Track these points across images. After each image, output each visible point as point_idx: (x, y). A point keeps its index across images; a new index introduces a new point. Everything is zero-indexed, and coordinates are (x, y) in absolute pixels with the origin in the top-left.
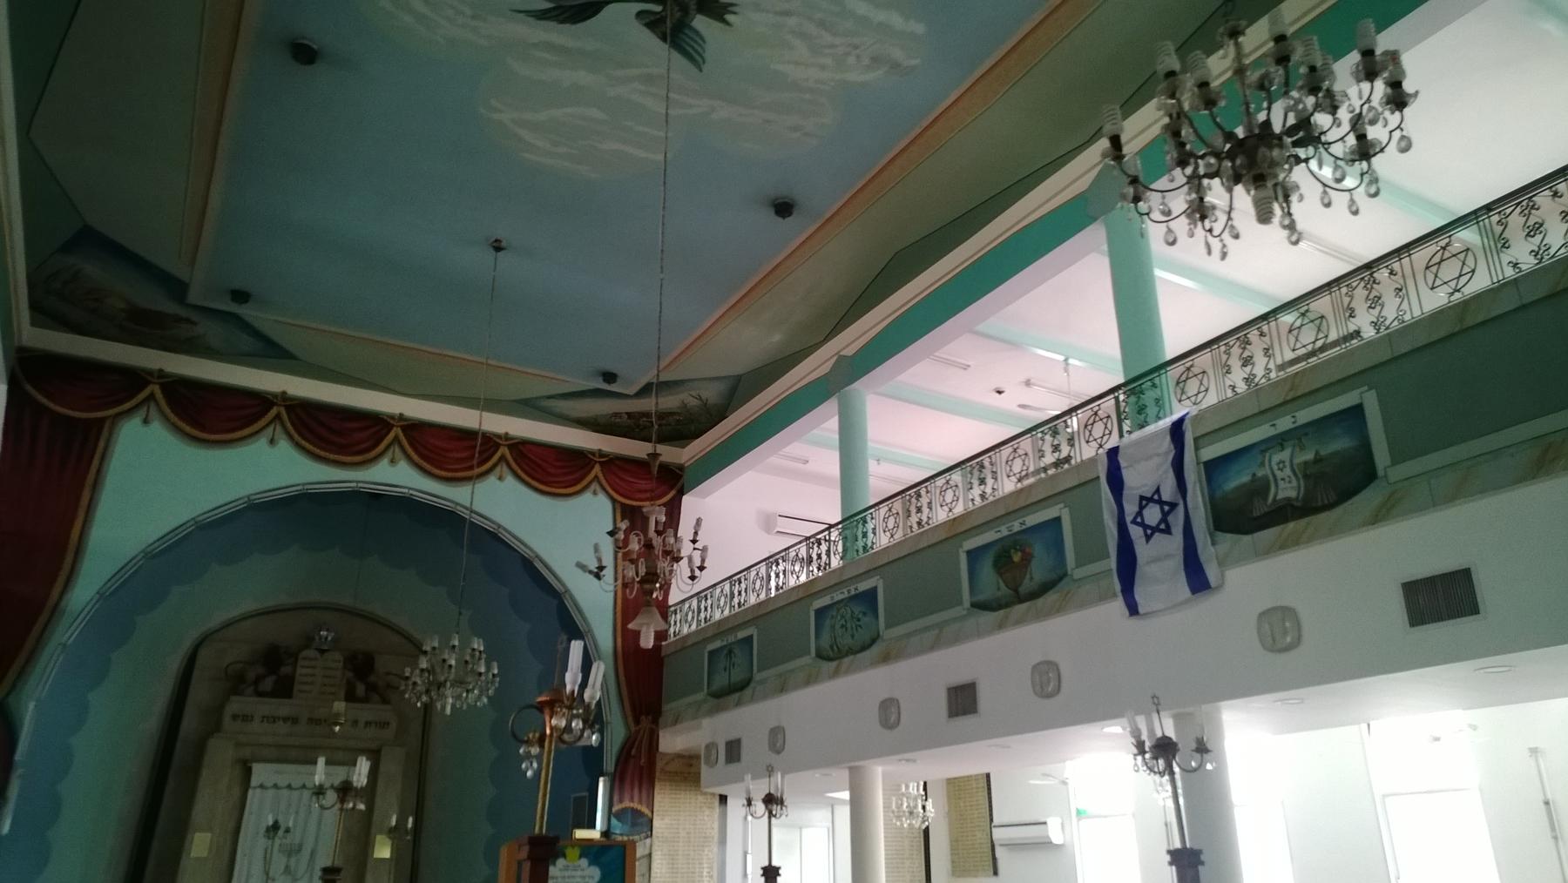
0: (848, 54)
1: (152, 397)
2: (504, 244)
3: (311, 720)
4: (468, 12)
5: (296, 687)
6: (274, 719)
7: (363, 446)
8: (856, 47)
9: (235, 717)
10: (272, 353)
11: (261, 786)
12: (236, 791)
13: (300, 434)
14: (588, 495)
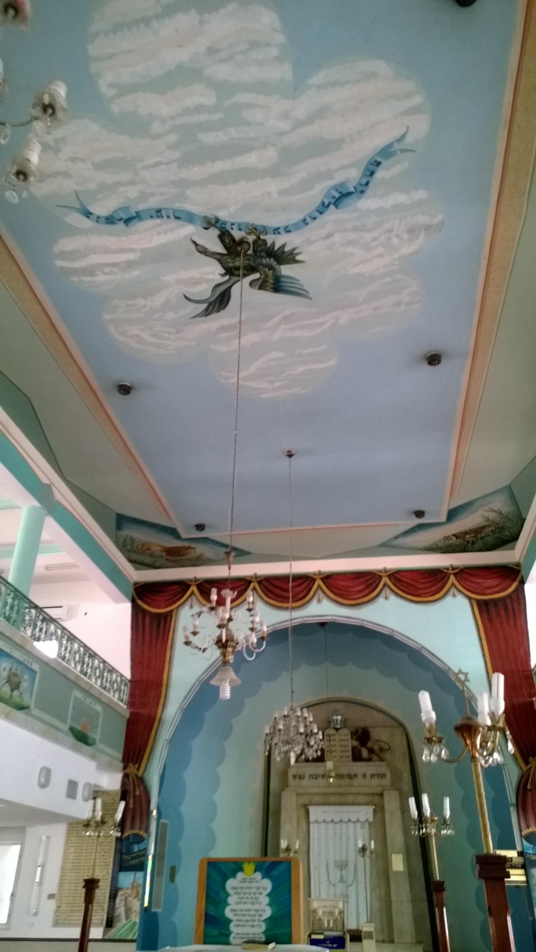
0: (389, 238)
1: (193, 593)
2: (293, 452)
4: (173, 330)
6: (315, 777)
7: (301, 596)
8: (390, 231)
9: (294, 777)
10: (242, 555)
11: (316, 821)
12: (304, 825)
13: (267, 596)
14: (449, 599)
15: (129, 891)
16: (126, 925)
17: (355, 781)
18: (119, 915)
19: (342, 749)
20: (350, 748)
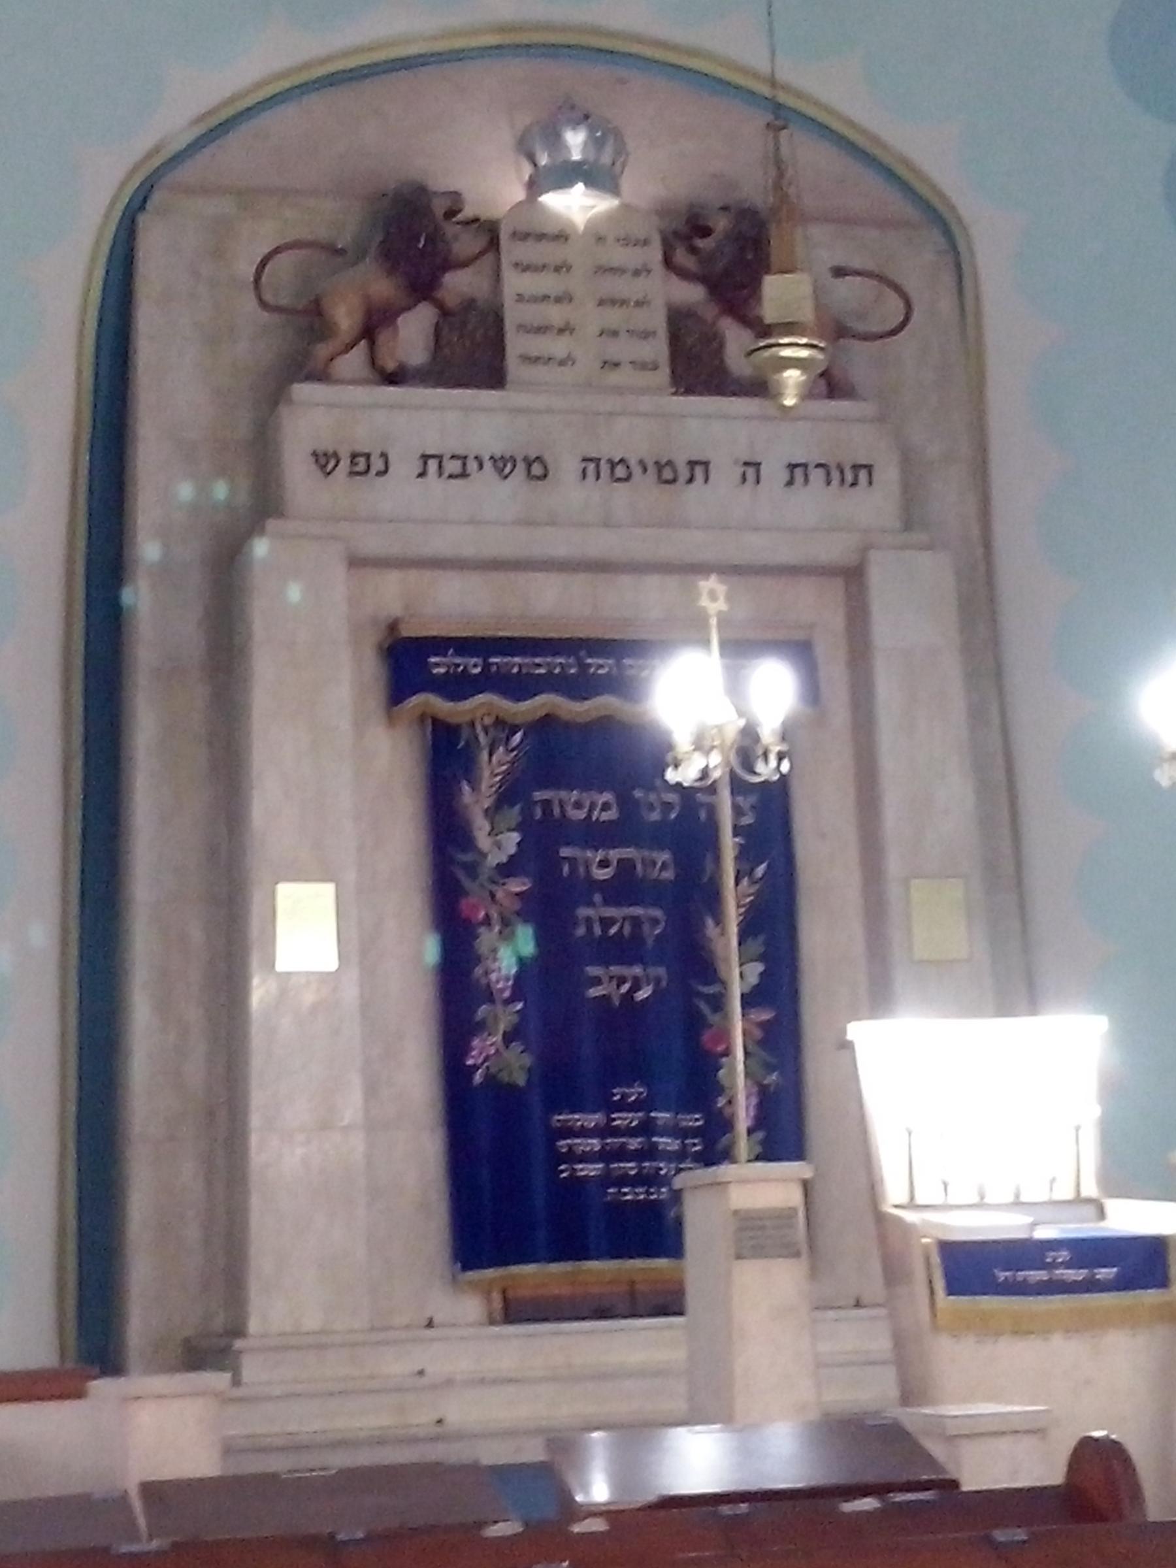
3: (591, 465)
5: (516, 345)
6: (459, 467)
9: (324, 461)
17: (694, 498)
19: (613, 317)
20: (658, 321)
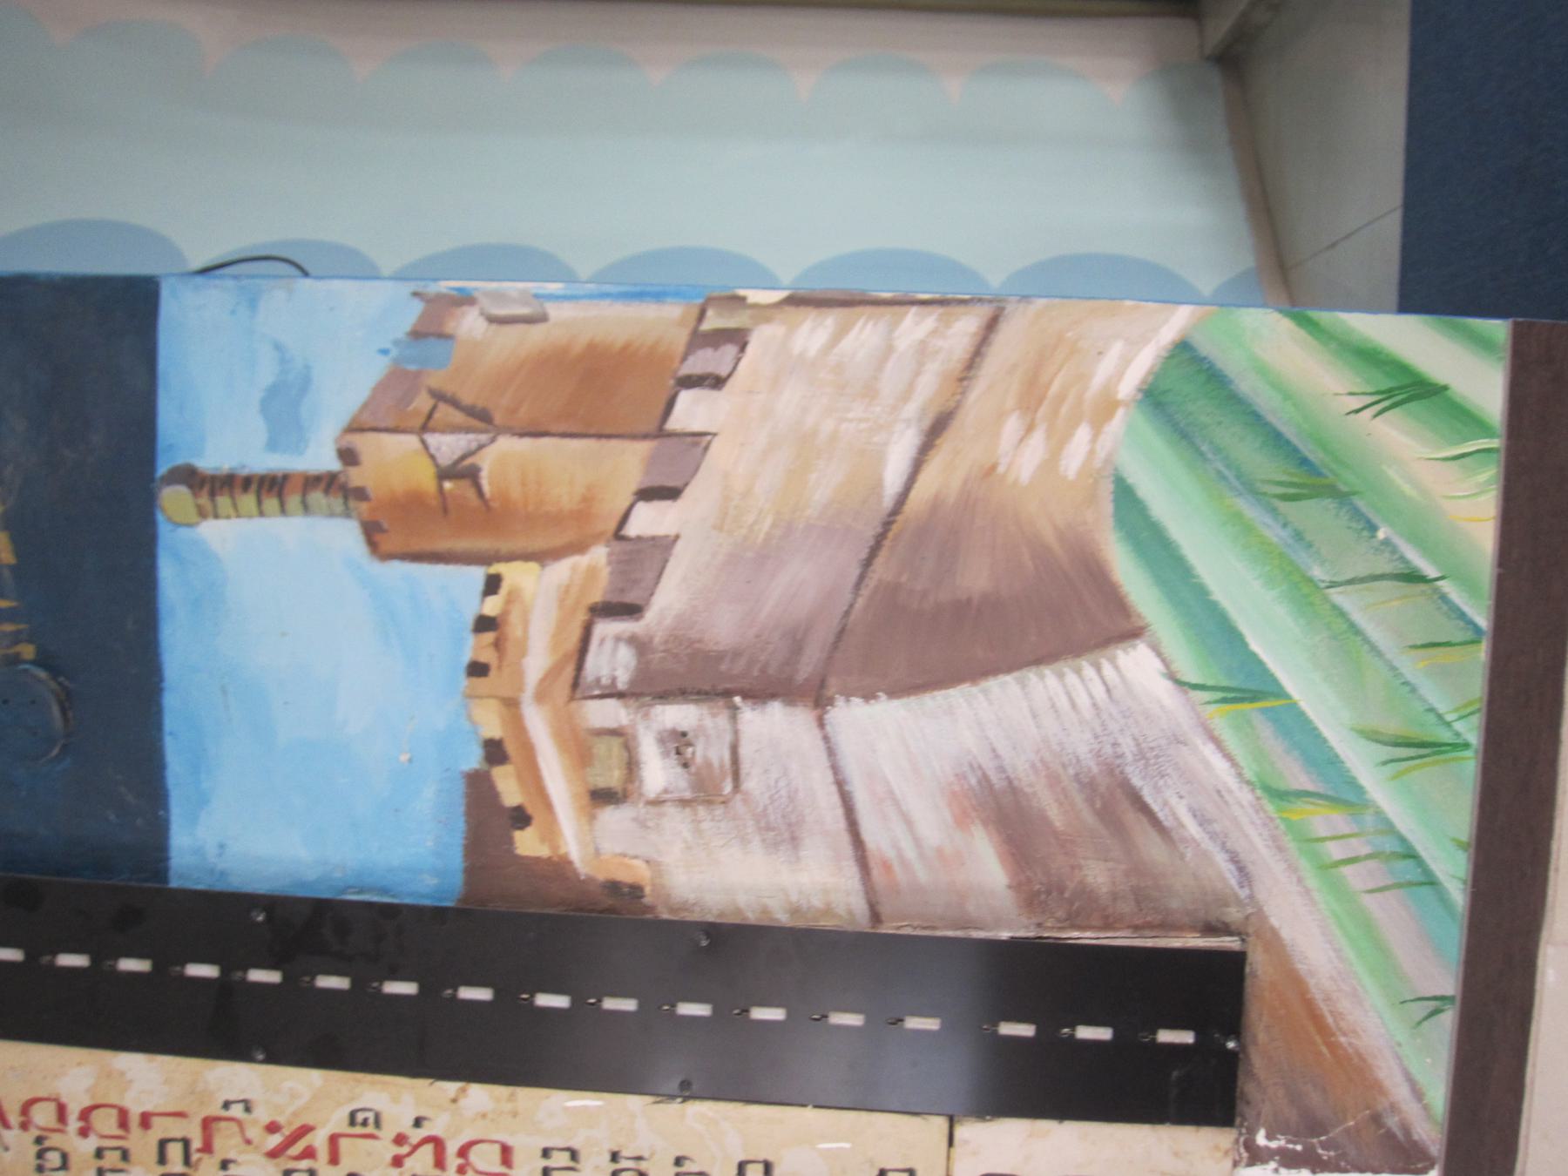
15: (542, 592)
16: (1216, 629)
18: (1003, 809)
